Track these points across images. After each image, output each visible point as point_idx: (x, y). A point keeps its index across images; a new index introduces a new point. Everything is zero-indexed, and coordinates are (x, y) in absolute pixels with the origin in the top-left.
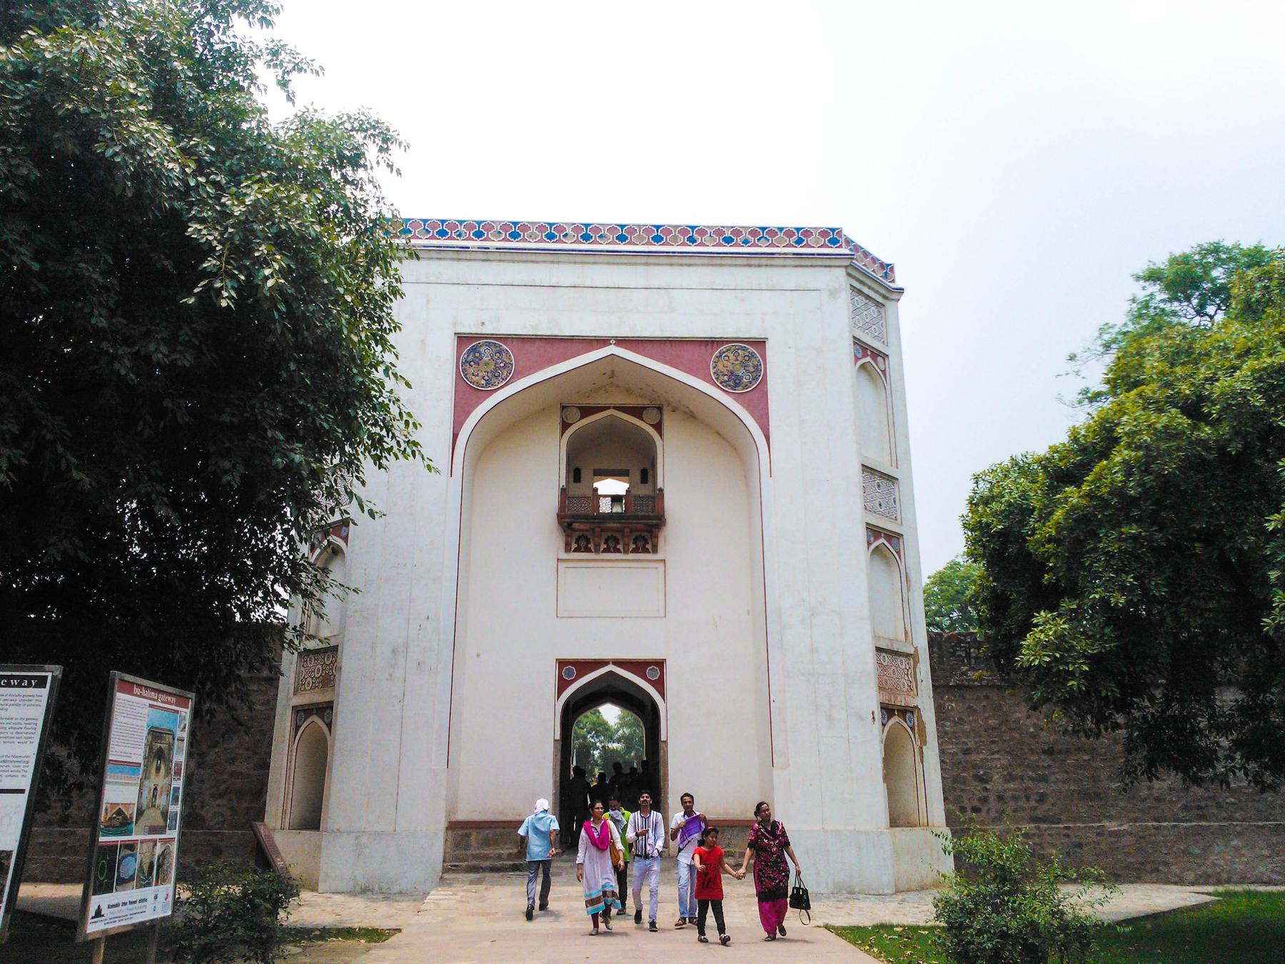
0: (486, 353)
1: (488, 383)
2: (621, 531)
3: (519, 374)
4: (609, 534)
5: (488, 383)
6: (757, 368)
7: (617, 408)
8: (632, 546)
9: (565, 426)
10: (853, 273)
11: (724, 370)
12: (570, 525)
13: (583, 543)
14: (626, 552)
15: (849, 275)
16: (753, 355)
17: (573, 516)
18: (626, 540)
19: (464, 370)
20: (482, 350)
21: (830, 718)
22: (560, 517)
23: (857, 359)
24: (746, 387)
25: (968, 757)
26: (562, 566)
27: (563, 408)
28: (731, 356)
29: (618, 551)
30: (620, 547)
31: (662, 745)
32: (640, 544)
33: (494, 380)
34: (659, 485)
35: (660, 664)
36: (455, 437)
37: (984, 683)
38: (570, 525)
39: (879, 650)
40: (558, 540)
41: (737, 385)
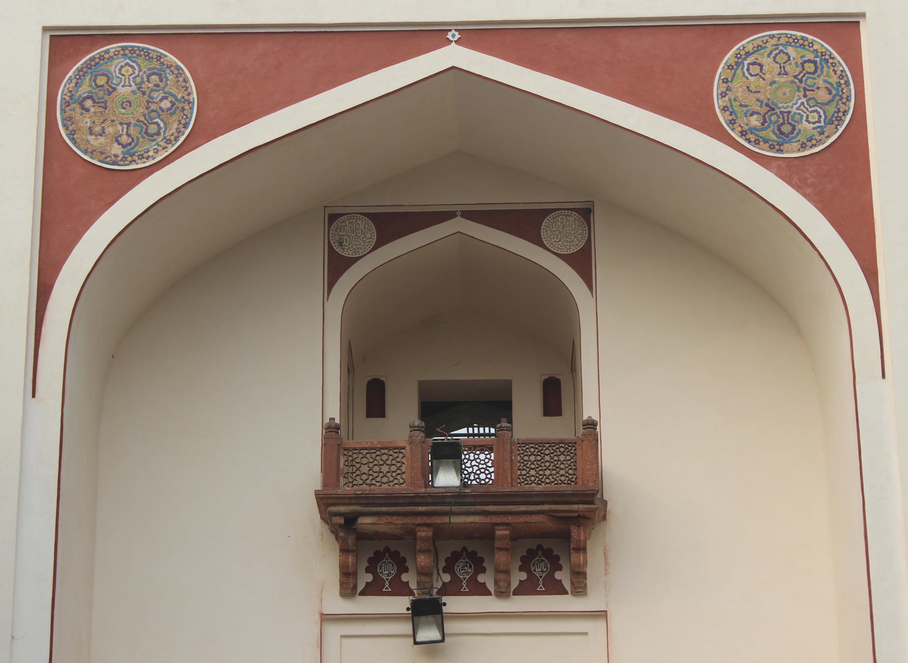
1: (130, 153)
2: (486, 535)
4: (457, 546)
5: (130, 153)
6: (837, 93)
8: (518, 577)
9: (337, 265)
11: (751, 100)
12: (350, 521)
13: (387, 572)
14: (502, 593)
16: (826, 58)
18: (501, 558)
19: (68, 120)
20: (114, 67)
22: (324, 501)
26: (334, 631)
27: (333, 218)
28: (767, 62)
29: (481, 590)
30: (486, 579)
34: (589, 411)
38: (350, 521)
40: (322, 562)
41: (784, 137)
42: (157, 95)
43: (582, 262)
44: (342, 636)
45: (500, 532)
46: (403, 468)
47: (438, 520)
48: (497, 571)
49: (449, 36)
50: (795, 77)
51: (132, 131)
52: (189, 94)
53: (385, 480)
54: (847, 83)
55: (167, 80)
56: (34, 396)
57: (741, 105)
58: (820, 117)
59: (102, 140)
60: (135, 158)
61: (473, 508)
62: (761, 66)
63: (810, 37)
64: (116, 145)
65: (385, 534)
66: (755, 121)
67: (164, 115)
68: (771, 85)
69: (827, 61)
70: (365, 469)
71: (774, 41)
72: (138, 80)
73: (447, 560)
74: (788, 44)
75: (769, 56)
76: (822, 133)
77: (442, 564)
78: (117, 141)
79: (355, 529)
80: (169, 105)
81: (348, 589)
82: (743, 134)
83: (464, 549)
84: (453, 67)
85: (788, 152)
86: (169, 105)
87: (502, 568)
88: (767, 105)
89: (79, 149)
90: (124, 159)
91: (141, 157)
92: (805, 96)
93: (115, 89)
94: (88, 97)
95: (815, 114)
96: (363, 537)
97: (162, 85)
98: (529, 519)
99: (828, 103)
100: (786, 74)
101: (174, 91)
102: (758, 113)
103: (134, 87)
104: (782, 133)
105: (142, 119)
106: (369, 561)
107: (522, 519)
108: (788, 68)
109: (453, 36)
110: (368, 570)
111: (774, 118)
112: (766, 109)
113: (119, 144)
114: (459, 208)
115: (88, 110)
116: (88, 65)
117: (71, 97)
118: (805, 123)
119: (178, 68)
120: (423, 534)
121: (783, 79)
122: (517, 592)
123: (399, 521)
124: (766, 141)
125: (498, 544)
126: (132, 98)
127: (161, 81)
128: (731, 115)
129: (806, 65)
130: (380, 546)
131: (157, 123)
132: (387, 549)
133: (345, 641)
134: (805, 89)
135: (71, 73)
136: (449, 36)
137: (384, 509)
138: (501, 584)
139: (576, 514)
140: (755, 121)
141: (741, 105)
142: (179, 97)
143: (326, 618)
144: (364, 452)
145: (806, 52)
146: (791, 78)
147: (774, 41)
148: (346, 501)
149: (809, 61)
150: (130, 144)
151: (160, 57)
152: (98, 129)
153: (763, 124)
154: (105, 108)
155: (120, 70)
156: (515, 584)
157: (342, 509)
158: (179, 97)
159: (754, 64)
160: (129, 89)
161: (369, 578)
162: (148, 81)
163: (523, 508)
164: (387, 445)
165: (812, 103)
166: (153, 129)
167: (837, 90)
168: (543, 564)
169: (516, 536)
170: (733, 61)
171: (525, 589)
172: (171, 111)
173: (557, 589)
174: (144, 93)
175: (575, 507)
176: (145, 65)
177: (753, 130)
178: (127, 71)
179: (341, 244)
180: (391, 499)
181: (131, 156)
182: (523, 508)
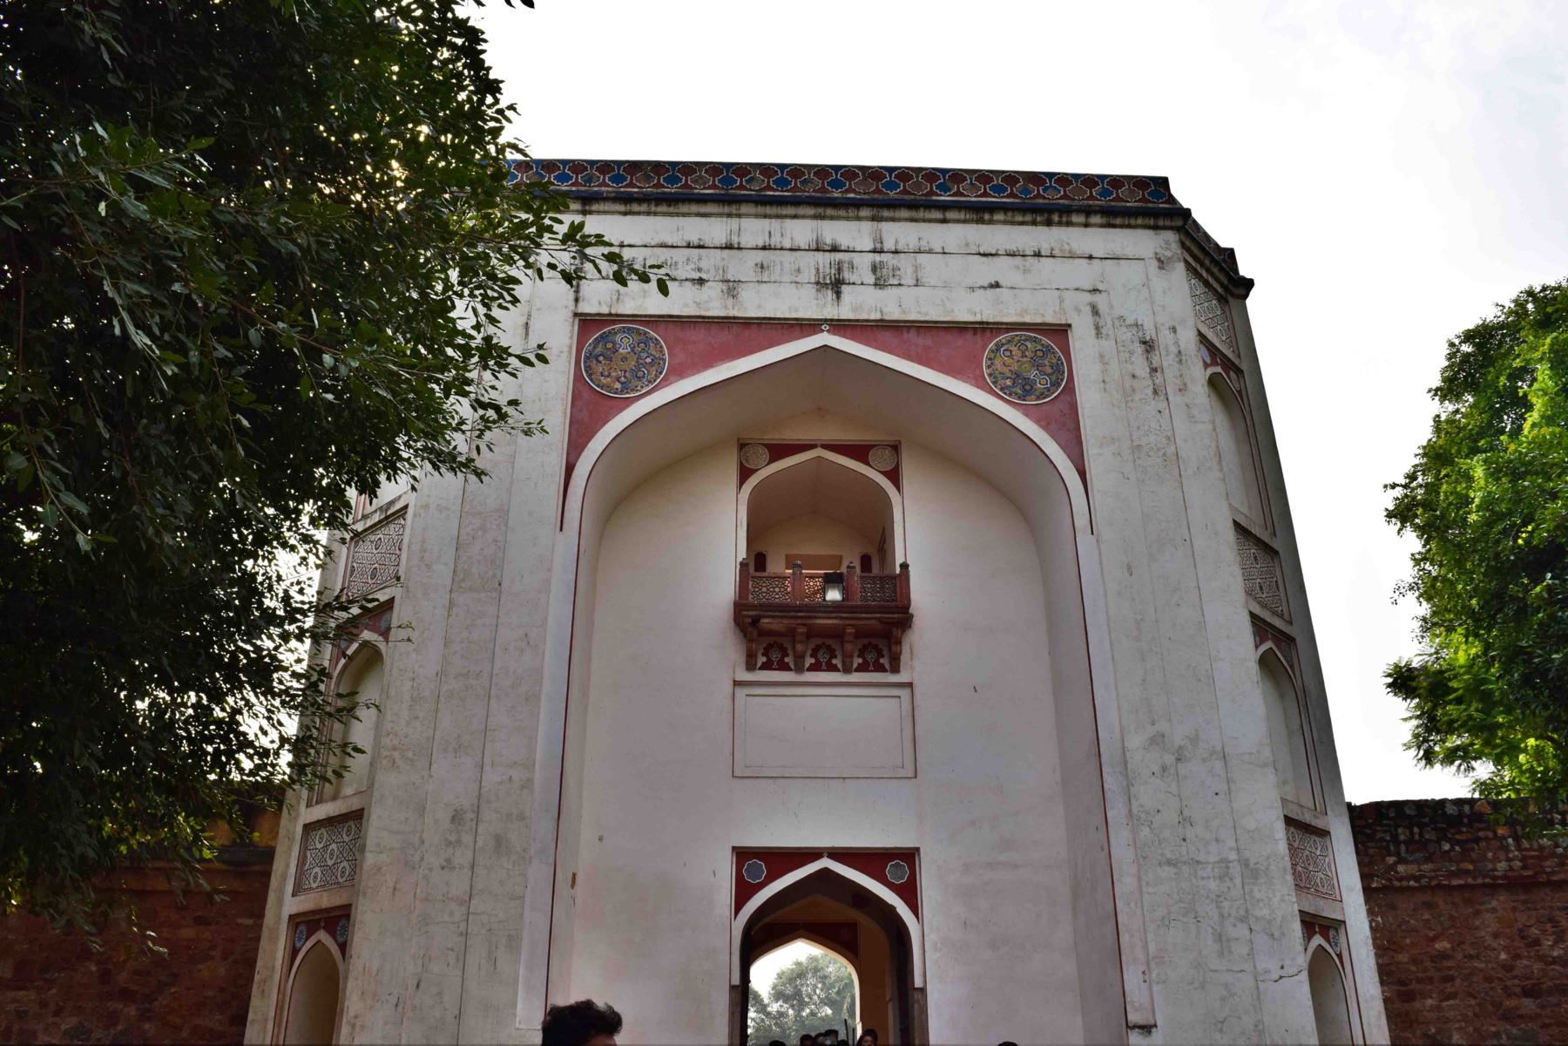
0: (624, 344)
2: (838, 634)
3: (679, 372)
4: (818, 641)
5: (626, 387)
6: (1057, 369)
9: (745, 474)
10: (1188, 243)
11: (1006, 370)
13: (775, 656)
14: (847, 670)
15: (1183, 245)
16: (1049, 349)
17: (762, 607)
18: (848, 647)
19: (588, 368)
20: (618, 338)
21: (1219, 937)
23: (1206, 366)
24: (1042, 396)
25: (1407, 1006)
26: (741, 693)
27: (742, 446)
28: (1015, 349)
29: (833, 668)
31: (917, 996)
33: (635, 382)
35: (909, 856)
36: (570, 469)
37: (1424, 881)
38: (755, 621)
39: (1289, 821)
42: (644, 355)
43: (894, 476)
66: (1008, 382)
81: (750, 666)
96: (764, 633)
122: (857, 670)
123: (786, 621)
130: (772, 640)
140: (1008, 382)
143: (736, 683)
169: (858, 635)
171: (861, 668)
173: (880, 668)
180: (783, 609)
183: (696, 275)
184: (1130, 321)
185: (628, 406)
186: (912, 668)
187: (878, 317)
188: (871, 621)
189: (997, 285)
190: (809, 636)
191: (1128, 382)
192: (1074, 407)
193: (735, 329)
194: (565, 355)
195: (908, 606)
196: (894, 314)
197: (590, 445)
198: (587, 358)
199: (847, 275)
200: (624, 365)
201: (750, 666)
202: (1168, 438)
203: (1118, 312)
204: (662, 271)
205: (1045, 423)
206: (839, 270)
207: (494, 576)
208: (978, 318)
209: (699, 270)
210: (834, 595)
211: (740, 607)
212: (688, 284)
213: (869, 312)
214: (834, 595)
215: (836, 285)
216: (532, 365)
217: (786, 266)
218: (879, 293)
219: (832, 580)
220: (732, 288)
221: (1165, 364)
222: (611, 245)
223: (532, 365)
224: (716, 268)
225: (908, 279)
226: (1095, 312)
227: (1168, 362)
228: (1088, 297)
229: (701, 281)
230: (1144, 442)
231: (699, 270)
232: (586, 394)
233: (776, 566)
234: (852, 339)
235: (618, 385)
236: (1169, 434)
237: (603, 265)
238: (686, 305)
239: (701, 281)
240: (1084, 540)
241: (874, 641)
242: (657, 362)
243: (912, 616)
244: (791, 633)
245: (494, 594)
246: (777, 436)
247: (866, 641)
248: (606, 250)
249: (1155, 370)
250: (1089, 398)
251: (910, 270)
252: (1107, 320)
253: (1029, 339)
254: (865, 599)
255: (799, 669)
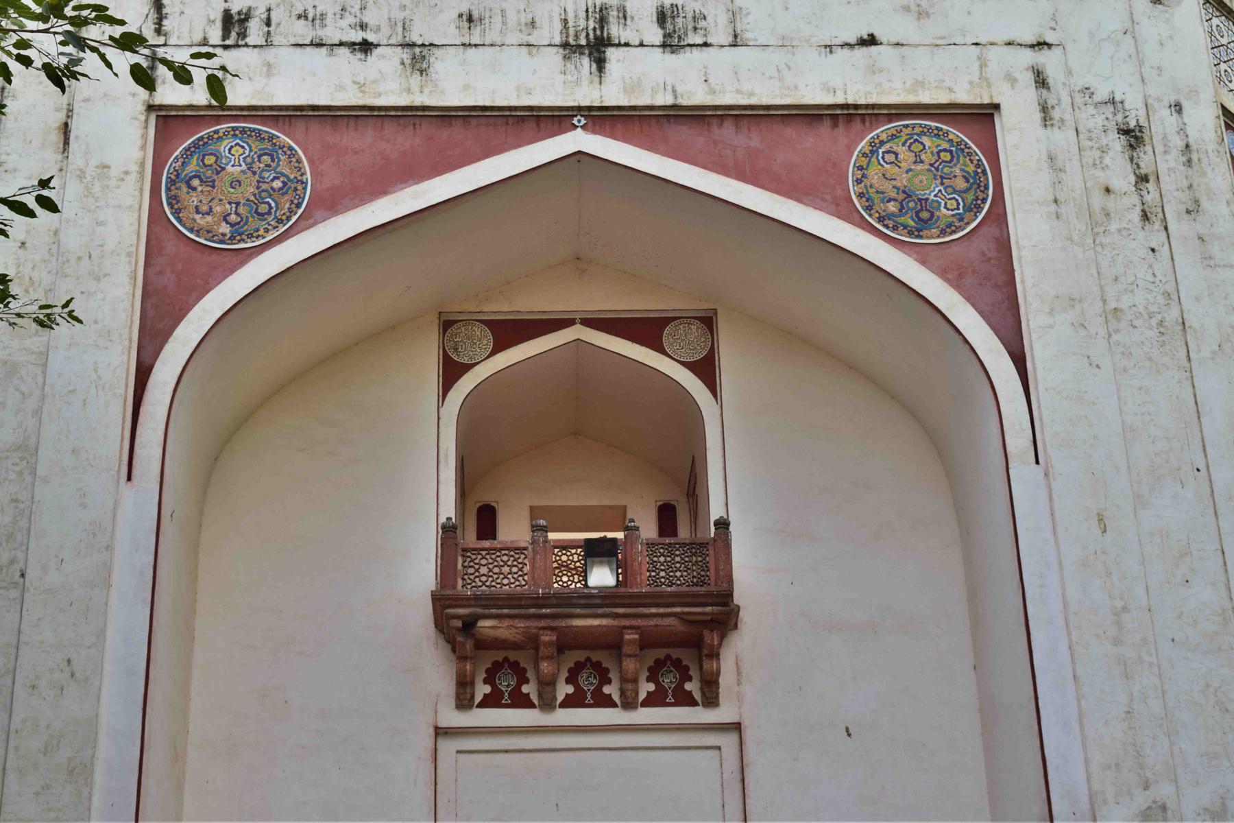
0: (234, 156)
2: (613, 643)
3: (331, 202)
4: (580, 655)
7: (590, 323)
8: (646, 688)
9: (452, 371)
11: (887, 186)
13: (506, 683)
16: (961, 148)
17: (478, 600)
18: (630, 665)
24: (949, 228)
26: (448, 747)
27: (447, 325)
28: (903, 152)
29: (607, 702)
32: (669, 681)
33: (254, 223)
36: (143, 374)
38: (469, 625)
40: (436, 672)
43: (706, 369)
44: (458, 752)
45: (627, 637)
46: (527, 569)
47: (562, 623)
48: (624, 680)
49: (575, 121)
50: (931, 165)
51: (241, 210)
52: (302, 175)
53: (506, 581)
54: (984, 172)
55: (279, 160)
56: (129, 478)
57: (877, 192)
58: (958, 204)
59: (209, 218)
60: (244, 237)
61: (600, 611)
62: (896, 154)
63: (944, 127)
64: (224, 224)
65: (504, 641)
66: (892, 207)
67: (275, 195)
68: (907, 172)
69: (962, 150)
70: (484, 570)
71: (909, 130)
72: (249, 160)
73: (570, 671)
74: (922, 133)
75: (904, 144)
76: (961, 220)
77: (564, 675)
78: (225, 220)
79: (473, 635)
80: (280, 185)
81: (464, 702)
82: (881, 220)
83: (588, 659)
84: (579, 152)
85: (928, 238)
86: (280, 185)
87: (630, 676)
88: (904, 192)
89: (184, 226)
90: (232, 238)
91: (250, 236)
92: (942, 184)
93: (223, 169)
94: (195, 176)
95: (954, 202)
96: (483, 645)
97: (274, 165)
98: (659, 621)
99: (967, 190)
100: (922, 162)
101: (286, 171)
102: (895, 200)
103: (244, 167)
104: (920, 219)
105: (252, 198)
106: (487, 671)
107: (653, 622)
108: (923, 157)
109: (579, 121)
110: (486, 681)
111: (912, 205)
112: (901, 196)
113: (227, 223)
114: (578, 316)
115: (194, 189)
116: (195, 145)
117: (177, 176)
118: (944, 211)
119: (291, 148)
120: (547, 638)
121: (920, 167)
122: (645, 704)
123: (521, 624)
124: (905, 227)
125: (626, 649)
126: (242, 178)
127: (273, 160)
128: (868, 200)
129: (942, 154)
130: (499, 656)
131: (268, 203)
132: (506, 659)
133: (460, 756)
134: (942, 177)
135: (177, 153)
136: (575, 121)
137: (506, 611)
138: (629, 694)
139: (709, 618)
140: (892, 207)
141: (877, 192)
142: (292, 177)
143: (440, 732)
144: (484, 553)
145: (941, 142)
146: (927, 167)
147: (909, 130)
148: (465, 602)
149: (945, 150)
150: (239, 223)
151: (272, 137)
152: (205, 208)
153: (900, 210)
154: (213, 187)
155: (230, 150)
156: (642, 696)
157: (461, 611)
158: (292, 177)
159: (888, 152)
160: (239, 169)
161: (487, 689)
162: (259, 161)
163: (653, 610)
164: (509, 545)
165: (949, 190)
166: (263, 208)
167: (974, 178)
168: (671, 675)
169: (646, 643)
170: (867, 150)
171: (654, 700)
172: (283, 190)
173: (686, 700)
174: (254, 173)
175: (709, 609)
176: (257, 146)
177: (891, 216)
178: (237, 151)
179: (456, 350)
180: (514, 603)
181: (240, 235)
182: (653, 610)
183: (357, 36)
184: (1102, 94)
185: (242, 263)
186: (740, 698)
187: (669, 100)
188: (667, 620)
189: (870, 41)
190: (562, 647)
191: (1098, 199)
192: (1004, 246)
193: (425, 128)
194: (134, 176)
195: (729, 594)
196: (695, 95)
197: (179, 331)
198: (172, 182)
199: (615, 30)
200: (236, 194)
201: (464, 702)
202: (1167, 295)
203: (1079, 82)
204: (215, 62)
205: (954, 276)
206: (603, 21)
207: (12, 562)
208: (840, 99)
209: (363, 26)
210: (602, 577)
211: (442, 602)
212: (344, 51)
213: (654, 91)
214: (602, 577)
215: (597, 48)
216: (31, 214)
217: (512, 17)
218: (670, 59)
219: (597, 551)
220: (418, 56)
221: (1162, 168)
222: (122, 23)
223: (31, 214)
224: (392, 24)
225: (720, 35)
226: (1041, 82)
227: (1163, 159)
228: (1029, 57)
229: (366, 47)
230: (1125, 303)
231: (363, 26)
232: (171, 247)
233: (514, 529)
234: (625, 140)
235: (225, 229)
236: (1170, 287)
237: (112, 53)
238: (341, 88)
239: (366, 47)
240: (1023, 473)
241: (675, 653)
242: (292, 186)
243: (738, 608)
244: (532, 642)
245: (15, 594)
246: (506, 308)
247: (660, 653)
248: (117, 31)
249: (1143, 179)
250: (1028, 230)
251: (723, 19)
252: (1060, 93)
253: (927, 131)
254: (655, 581)
255: (547, 705)
